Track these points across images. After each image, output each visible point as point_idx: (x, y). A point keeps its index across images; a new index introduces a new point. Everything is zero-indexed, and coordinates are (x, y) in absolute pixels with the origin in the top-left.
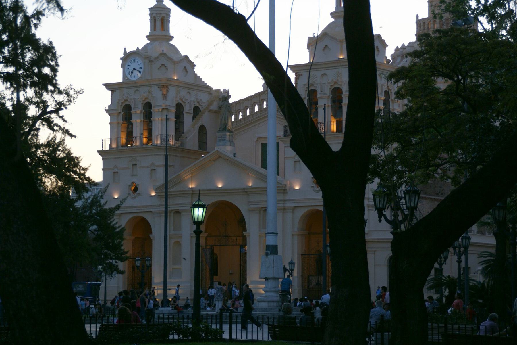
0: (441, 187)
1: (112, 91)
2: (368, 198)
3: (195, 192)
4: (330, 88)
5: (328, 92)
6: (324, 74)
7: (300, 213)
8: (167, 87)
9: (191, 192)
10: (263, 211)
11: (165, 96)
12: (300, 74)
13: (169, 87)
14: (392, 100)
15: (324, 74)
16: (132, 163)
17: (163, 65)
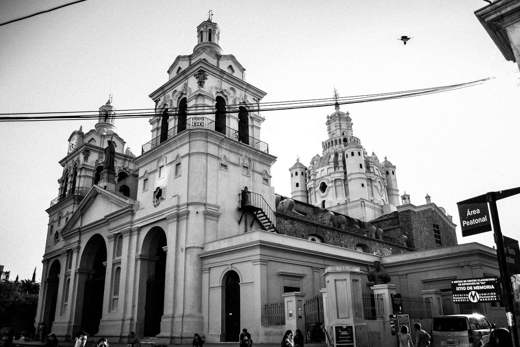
0: (321, 218)
1: (64, 166)
2: (205, 204)
3: (81, 230)
4: (178, 101)
5: (175, 105)
6: (175, 91)
7: (144, 233)
8: (88, 151)
9: (78, 230)
10: (119, 238)
11: (86, 159)
12: (158, 100)
13: (91, 152)
14: (251, 117)
15: (175, 91)
16: (59, 216)
17: (93, 139)
